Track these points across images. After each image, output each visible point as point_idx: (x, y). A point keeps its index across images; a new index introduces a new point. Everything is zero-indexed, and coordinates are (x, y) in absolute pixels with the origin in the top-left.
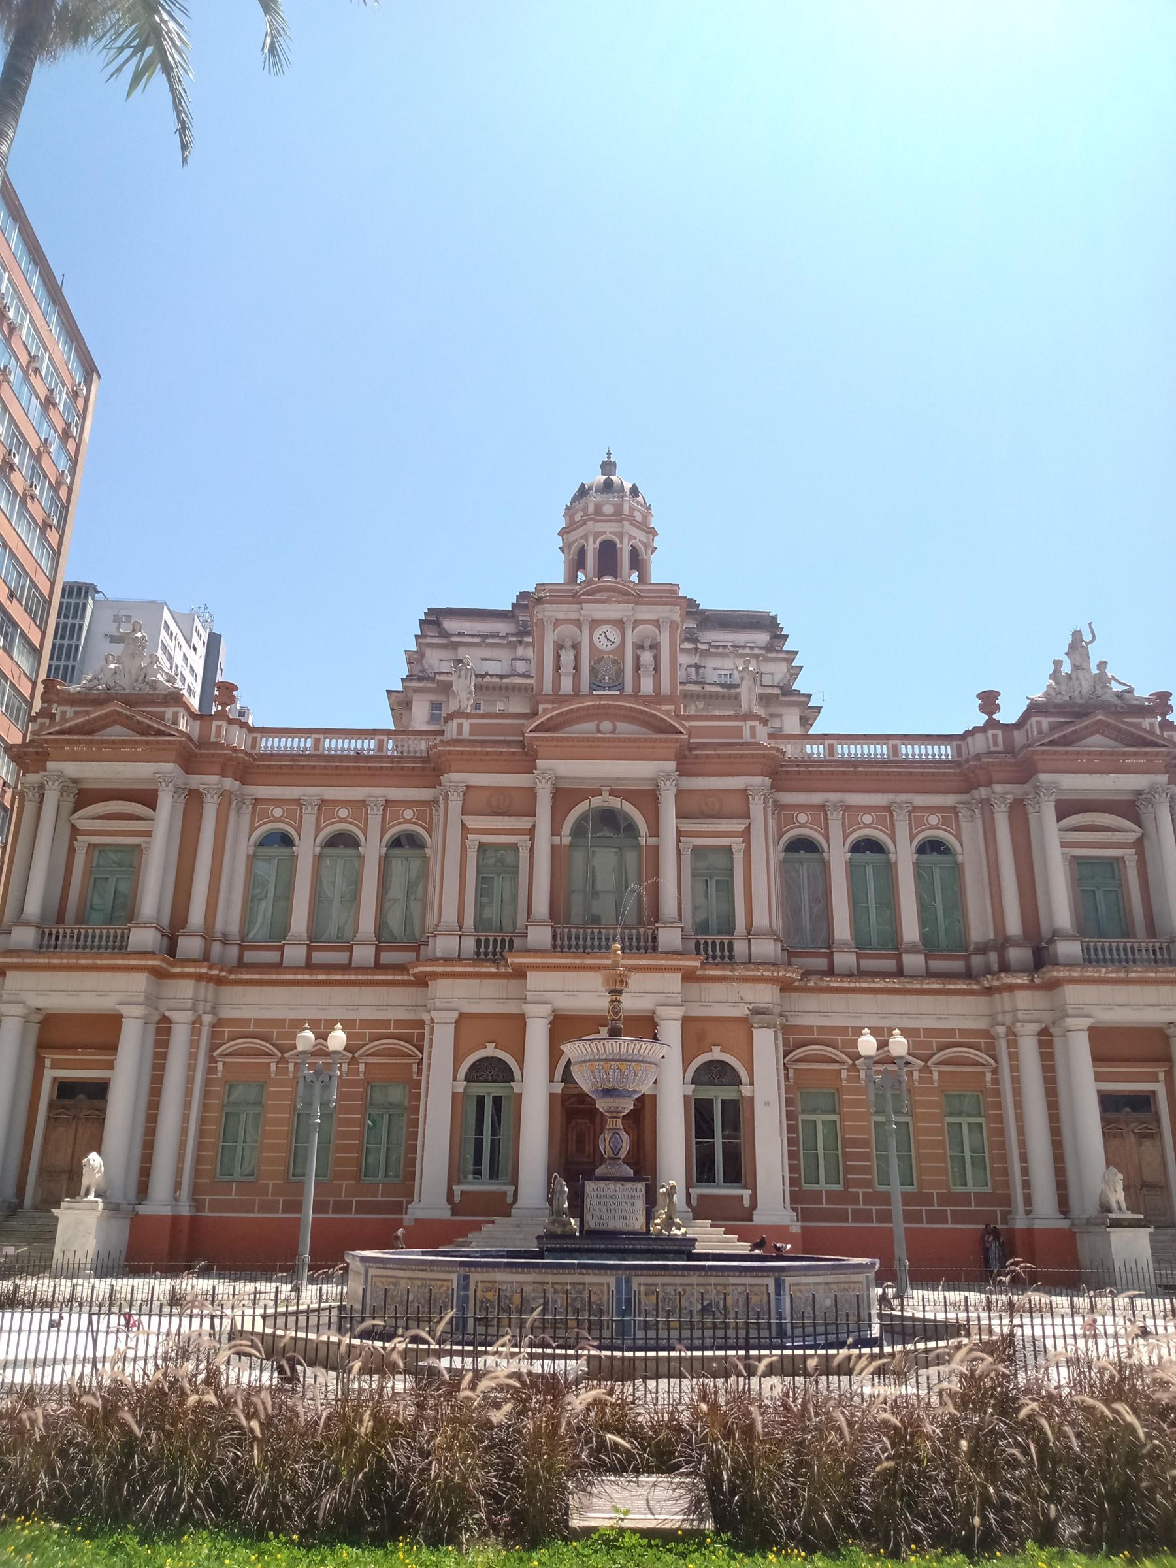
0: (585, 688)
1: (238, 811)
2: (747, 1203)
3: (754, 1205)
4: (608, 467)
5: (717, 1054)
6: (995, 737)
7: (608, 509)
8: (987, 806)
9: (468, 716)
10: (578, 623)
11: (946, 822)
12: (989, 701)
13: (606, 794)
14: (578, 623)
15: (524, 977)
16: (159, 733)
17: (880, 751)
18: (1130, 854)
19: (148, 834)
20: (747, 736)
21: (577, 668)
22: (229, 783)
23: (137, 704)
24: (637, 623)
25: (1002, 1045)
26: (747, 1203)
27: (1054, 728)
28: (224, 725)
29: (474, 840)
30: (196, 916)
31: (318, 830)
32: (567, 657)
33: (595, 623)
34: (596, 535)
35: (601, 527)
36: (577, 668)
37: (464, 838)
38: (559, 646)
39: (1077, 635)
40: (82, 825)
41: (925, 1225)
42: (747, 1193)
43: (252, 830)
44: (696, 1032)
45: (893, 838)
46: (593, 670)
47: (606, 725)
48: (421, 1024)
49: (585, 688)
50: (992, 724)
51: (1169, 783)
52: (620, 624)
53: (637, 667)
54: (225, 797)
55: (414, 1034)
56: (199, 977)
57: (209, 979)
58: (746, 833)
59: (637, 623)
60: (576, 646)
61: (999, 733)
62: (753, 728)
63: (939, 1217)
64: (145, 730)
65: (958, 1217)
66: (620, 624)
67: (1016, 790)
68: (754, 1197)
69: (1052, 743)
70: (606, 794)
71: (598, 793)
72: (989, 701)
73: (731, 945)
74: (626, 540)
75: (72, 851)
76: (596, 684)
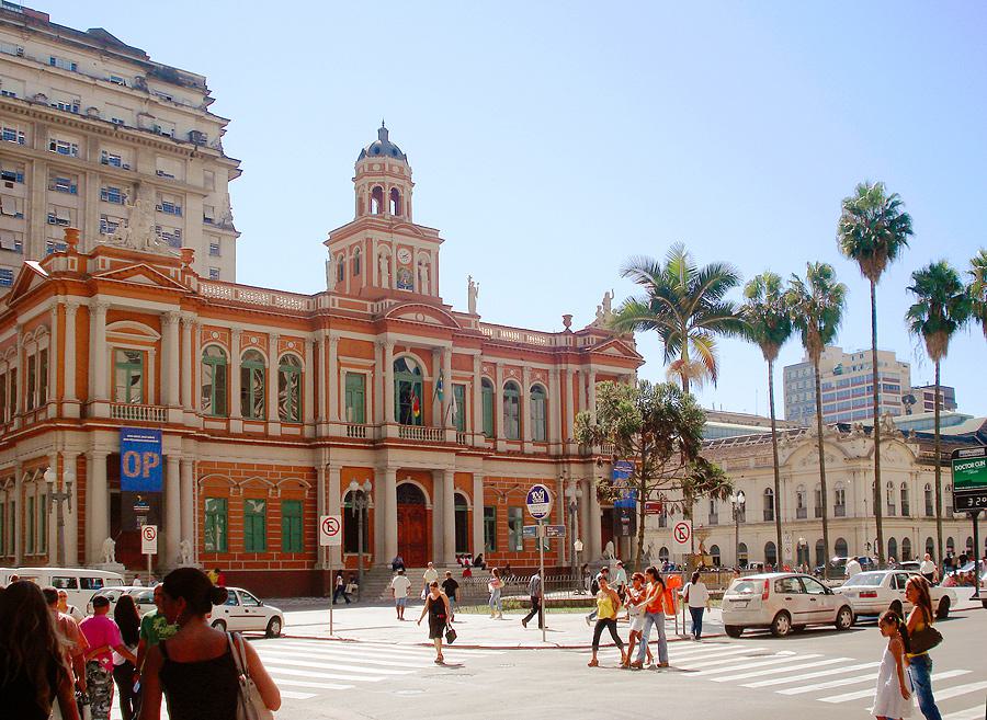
4: (383, 133)
8: (563, 373)
10: (390, 244)
12: (567, 319)
14: (390, 244)
17: (515, 337)
31: (241, 350)
32: (384, 266)
35: (394, 180)
39: (607, 294)
43: (202, 346)
45: (522, 382)
47: (420, 317)
50: (568, 332)
52: (411, 248)
60: (389, 258)
64: (162, 281)
66: (411, 248)
72: (567, 319)
76: (400, 285)
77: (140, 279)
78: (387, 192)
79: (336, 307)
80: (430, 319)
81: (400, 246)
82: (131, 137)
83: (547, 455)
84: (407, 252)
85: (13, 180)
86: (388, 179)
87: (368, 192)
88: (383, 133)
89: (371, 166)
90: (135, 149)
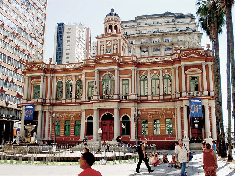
0: (105, 54)
1: (54, 79)
2: (130, 138)
3: (131, 138)
4: (113, 10)
5: (125, 114)
6: (176, 55)
7: (110, 19)
8: (175, 68)
9: (86, 60)
11: (169, 71)
13: (108, 72)
15: (93, 104)
16: (40, 68)
18: (200, 75)
19: (40, 84)
20: (132, 60)
21: (104, 50)
22: (52, 75)
23: (37, 64)
24: (113, 40)
25: (175, 110)
26: (130, 138)
27: (185, 53)
28: (50, 65)
29: (87, 81)
30: (48, 97)
33: (107, 41)
34: (108, 24)
35: (109, 22)
36: (104, 50)
37: (86, 81)
38: (101, 46)
40: (33, 83)
41: (153, 141)
42: (129, 136)
44: (121, 111)
46: (106, 50)
47: (106, 61)
48: (80, 111)
49: (105, 54)
51: (206, 62)
52: (110, 41)
53: (114, 48)
54: (52, 77)
55: (80, 112)
56: (49, 106)
57: (51, 106)
58: (131, 77)
59: (113, 40)
61: (177, 54)
62: (133, 58)
63: (164, 139)
65: (167, 139)
66: (110, 41)
67: (179, 65)
68: (131, 137)
69: (183, 57)
70: (108, 72)
71: (107, 72)
73: (128, 96)
74: (113, 24)
75: (31, 87)
76: (107, 53)
77: (35, 68)
78: (113, 26)
79: (86, 64)
80: (109, 61)
81: (107, 41)
82: (170, 34)
83: (170, 99)
84: (109, 42)
85: (146, 51)
86: (113, 22)
87: (108, 26)
88: (113, 10)
89: (109, 19)
90: (172, 36)
